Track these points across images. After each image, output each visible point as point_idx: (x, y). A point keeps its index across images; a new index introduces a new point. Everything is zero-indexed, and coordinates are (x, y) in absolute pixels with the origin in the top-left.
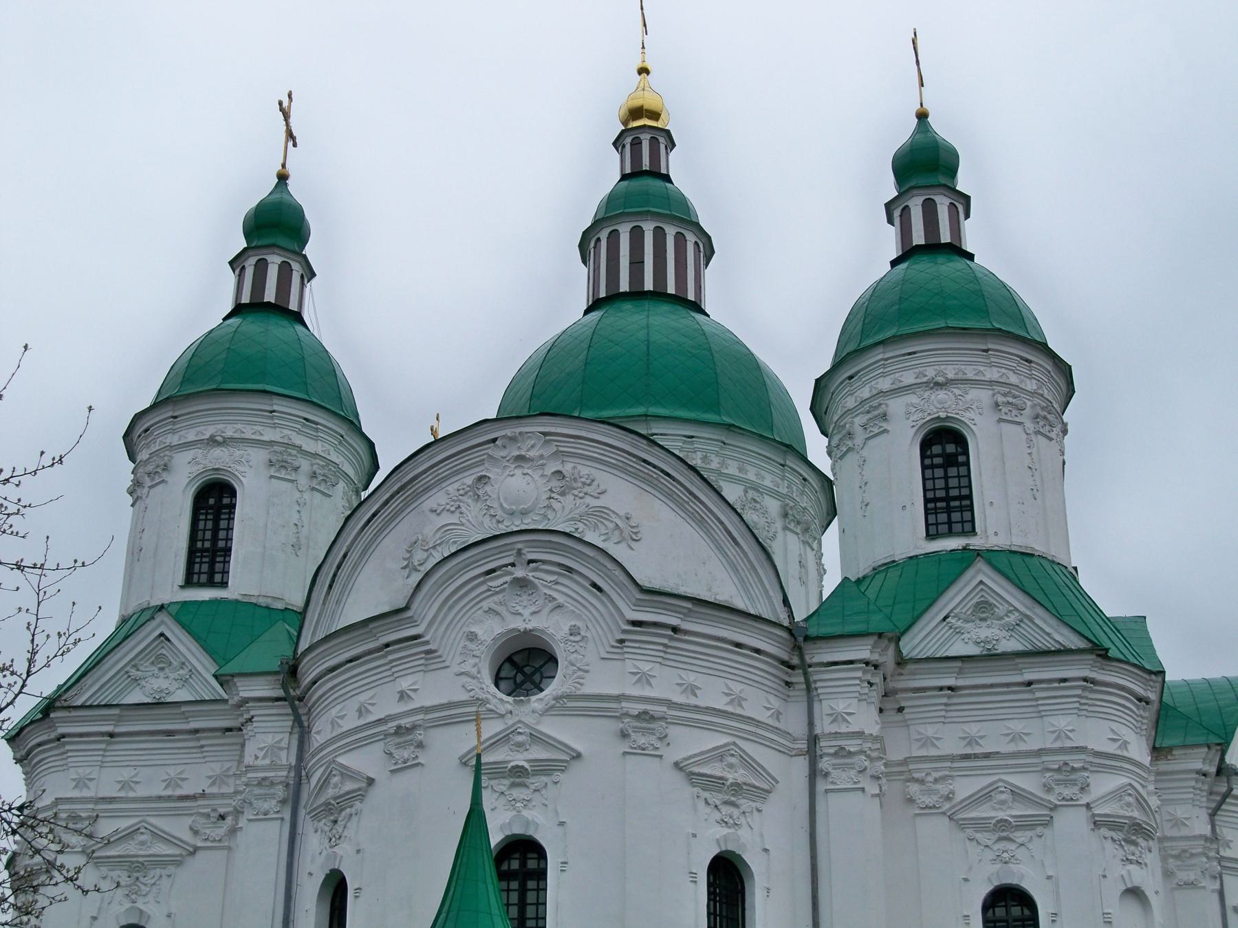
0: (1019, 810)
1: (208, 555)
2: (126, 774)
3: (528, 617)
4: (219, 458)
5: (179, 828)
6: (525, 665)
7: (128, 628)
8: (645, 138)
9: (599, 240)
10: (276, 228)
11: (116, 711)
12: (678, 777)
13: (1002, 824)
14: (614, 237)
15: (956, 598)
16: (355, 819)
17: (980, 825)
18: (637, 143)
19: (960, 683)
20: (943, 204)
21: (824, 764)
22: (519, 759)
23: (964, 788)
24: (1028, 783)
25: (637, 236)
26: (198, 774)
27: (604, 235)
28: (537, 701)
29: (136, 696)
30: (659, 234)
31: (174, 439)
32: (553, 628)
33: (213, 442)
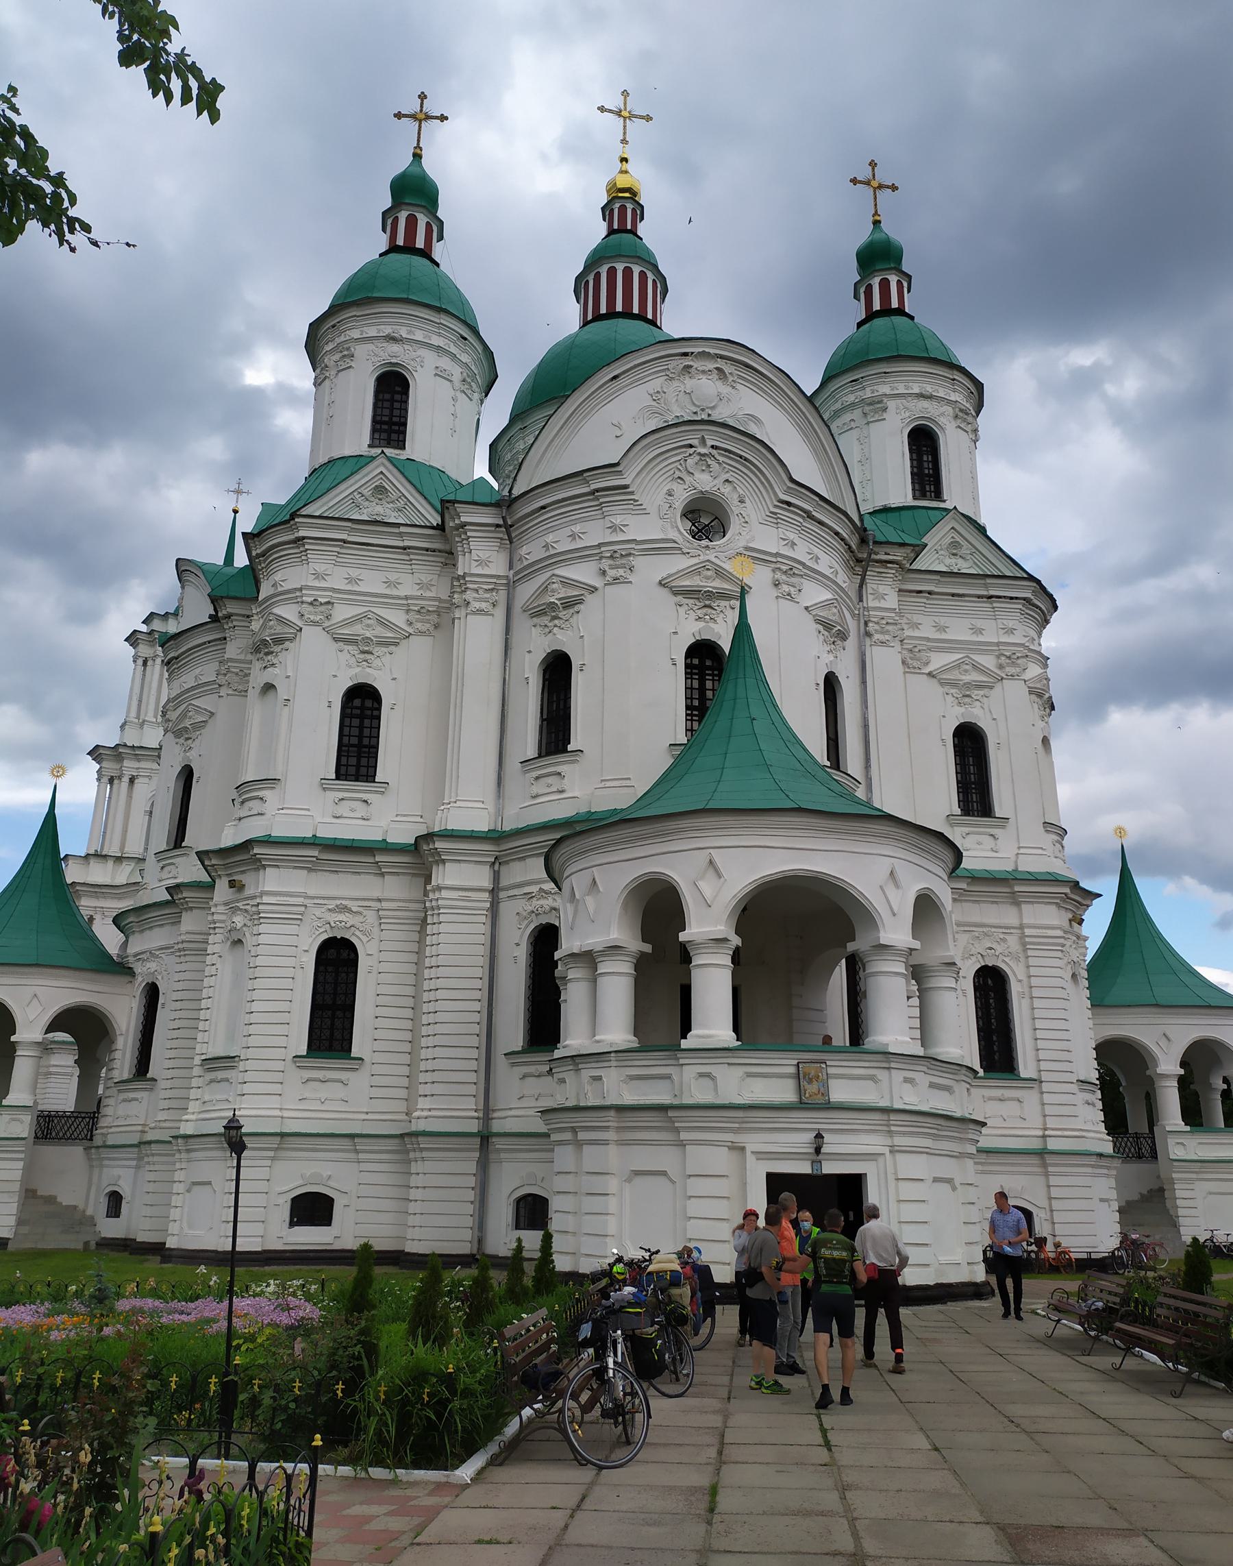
0: (975, 677)
2: (354, 573)
5: (398, 618)
9: (598, 276)
11: (349, 524)
12: (808, 619)
13: (968, 685)
14: (612, 272)
16: (575, 616)
17: (953, 684)
19: (936, 590)
20: (893, 279)
21: (872, 627)
25: (628, 273)
26: (415, 581)
27: (604, 271)
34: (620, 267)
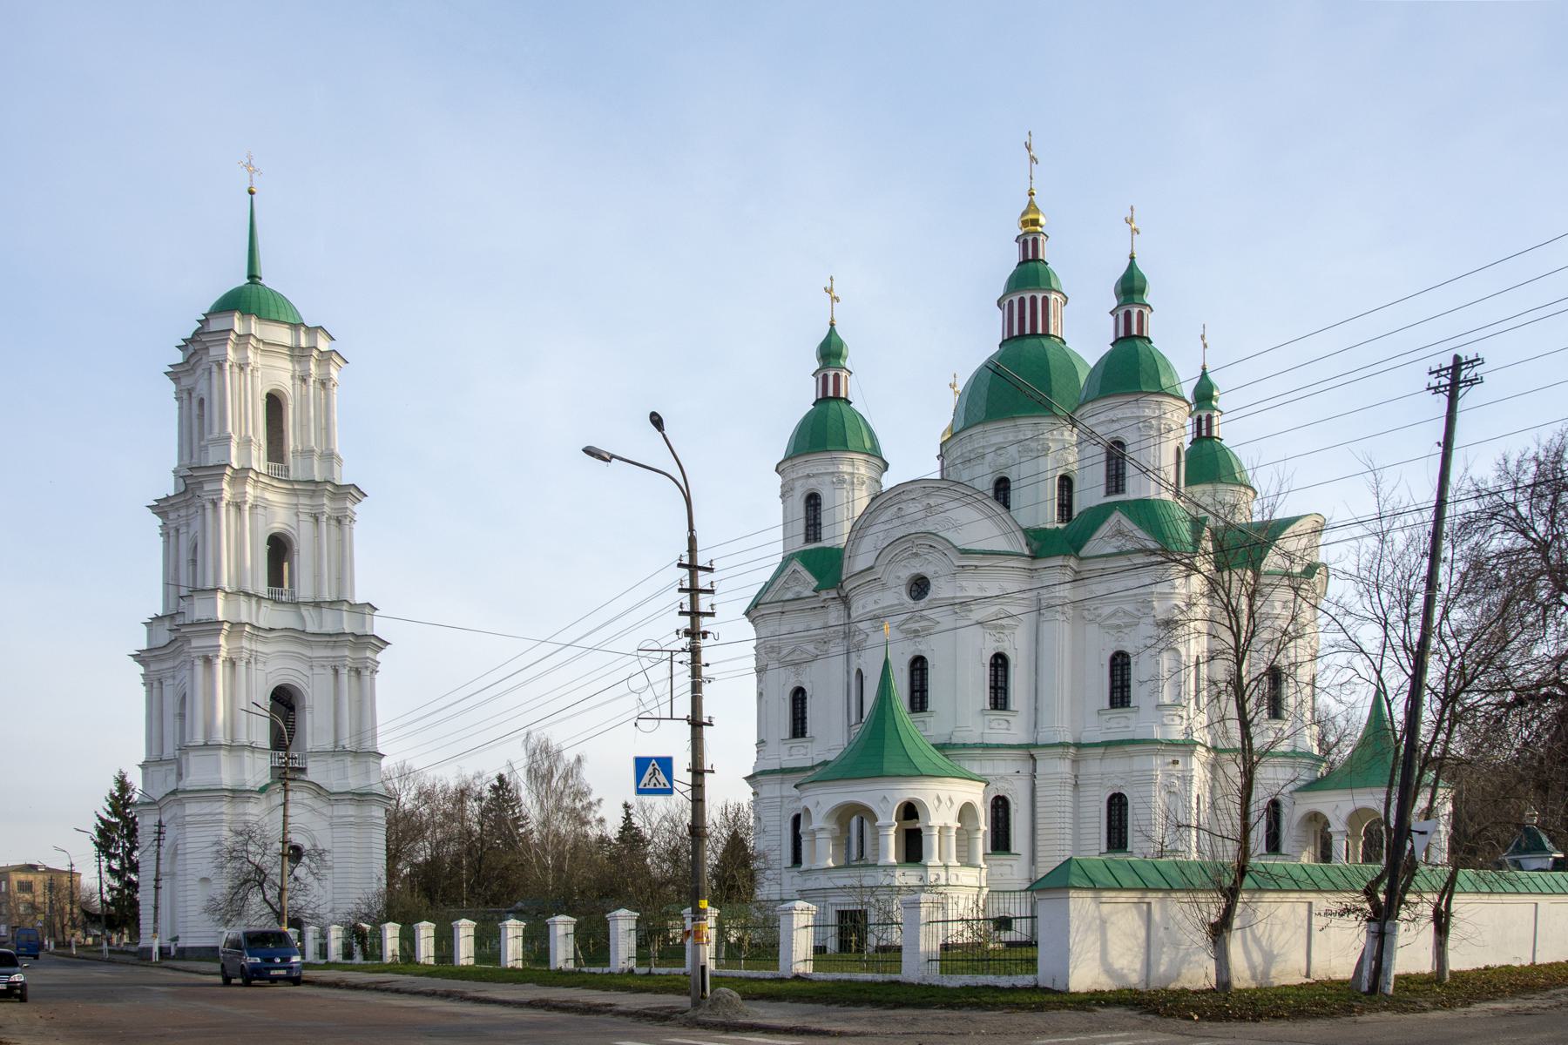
1: (813, 527)
3: (917, 568)
4: (813, 484)
6: (919, 587)
7: (787, 560)
8: (1030, 238)
10: (831, 352)
15: (1105, 529)
18: (1025, 242)
22: (916, 626)
23: (1107, 610)
24: (1128, 607)
28: (922, 603)
29: (789, 595)
30: (1034, 299)
31: (794, 476)
32: (927, 570)
33: (808, 476)
34: (1016, 299)
